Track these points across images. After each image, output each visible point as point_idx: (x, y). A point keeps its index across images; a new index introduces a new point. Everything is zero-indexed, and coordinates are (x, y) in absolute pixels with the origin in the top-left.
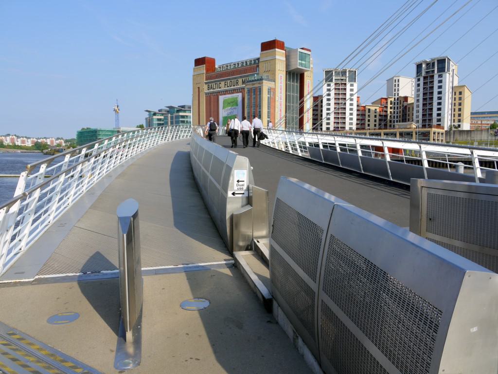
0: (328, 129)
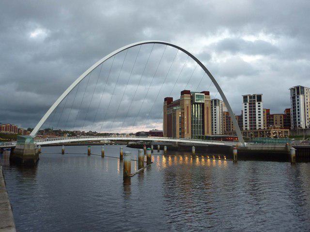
0: (246, 129)
